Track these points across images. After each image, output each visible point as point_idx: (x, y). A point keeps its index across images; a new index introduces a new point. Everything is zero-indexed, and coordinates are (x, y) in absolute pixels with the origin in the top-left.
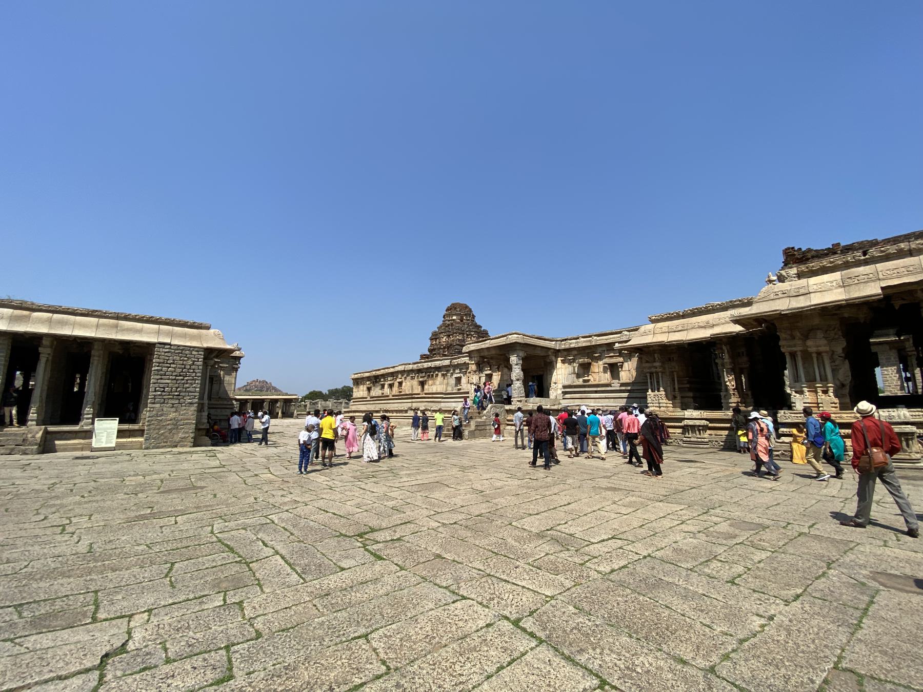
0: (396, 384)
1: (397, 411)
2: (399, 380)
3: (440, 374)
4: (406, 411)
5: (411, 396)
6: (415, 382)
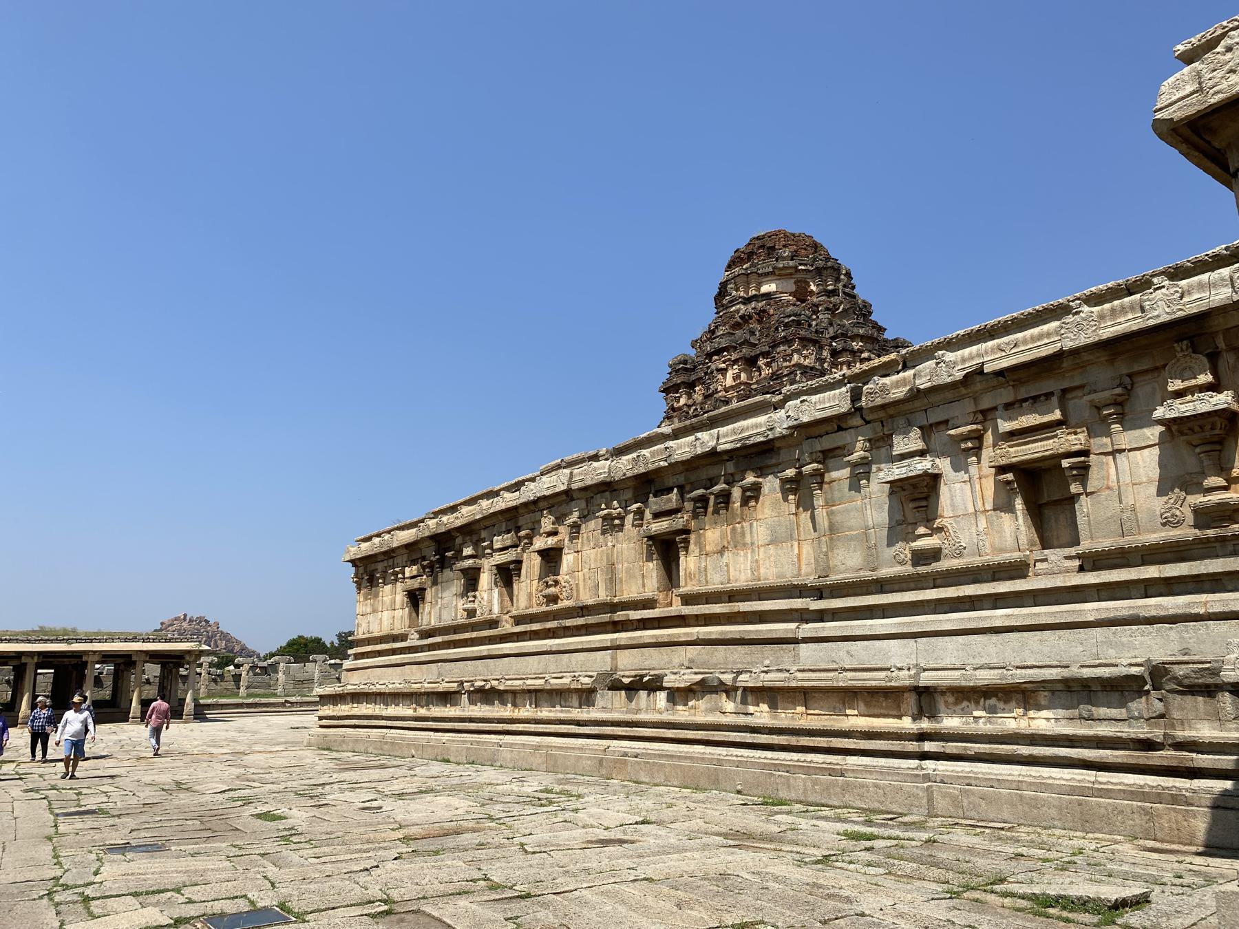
0: (532, 563)
1: (537, 696)
2: (540, 543)
3: (770, 485)
4: (586, 696)
5: (608, 617)
6: (627, 546)
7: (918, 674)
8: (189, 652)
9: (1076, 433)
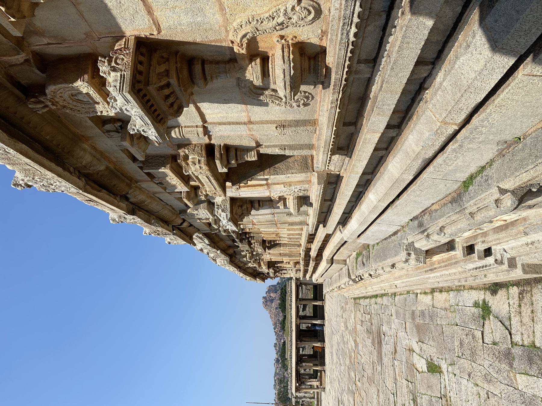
7: (416, 250)
8: (296, 284)
9: (186, 157)
